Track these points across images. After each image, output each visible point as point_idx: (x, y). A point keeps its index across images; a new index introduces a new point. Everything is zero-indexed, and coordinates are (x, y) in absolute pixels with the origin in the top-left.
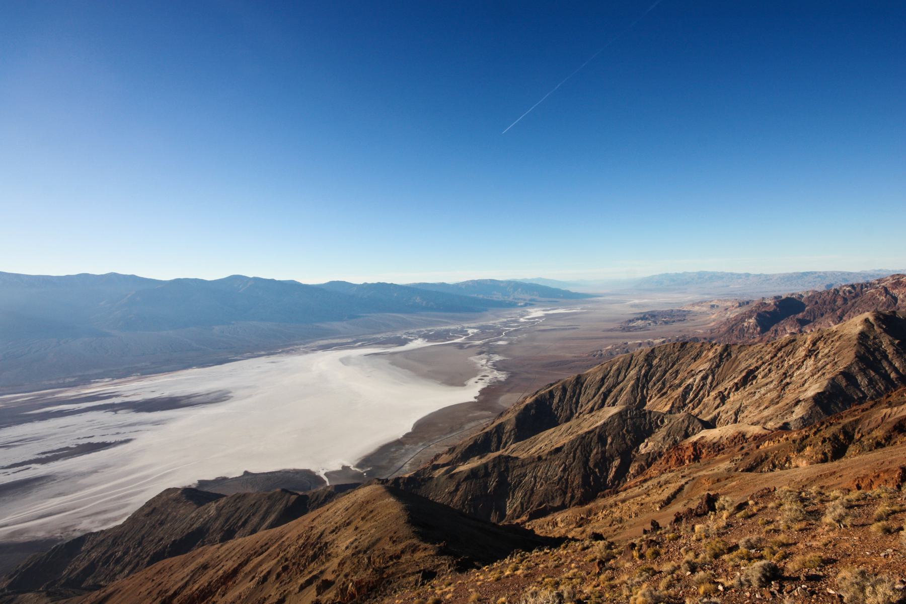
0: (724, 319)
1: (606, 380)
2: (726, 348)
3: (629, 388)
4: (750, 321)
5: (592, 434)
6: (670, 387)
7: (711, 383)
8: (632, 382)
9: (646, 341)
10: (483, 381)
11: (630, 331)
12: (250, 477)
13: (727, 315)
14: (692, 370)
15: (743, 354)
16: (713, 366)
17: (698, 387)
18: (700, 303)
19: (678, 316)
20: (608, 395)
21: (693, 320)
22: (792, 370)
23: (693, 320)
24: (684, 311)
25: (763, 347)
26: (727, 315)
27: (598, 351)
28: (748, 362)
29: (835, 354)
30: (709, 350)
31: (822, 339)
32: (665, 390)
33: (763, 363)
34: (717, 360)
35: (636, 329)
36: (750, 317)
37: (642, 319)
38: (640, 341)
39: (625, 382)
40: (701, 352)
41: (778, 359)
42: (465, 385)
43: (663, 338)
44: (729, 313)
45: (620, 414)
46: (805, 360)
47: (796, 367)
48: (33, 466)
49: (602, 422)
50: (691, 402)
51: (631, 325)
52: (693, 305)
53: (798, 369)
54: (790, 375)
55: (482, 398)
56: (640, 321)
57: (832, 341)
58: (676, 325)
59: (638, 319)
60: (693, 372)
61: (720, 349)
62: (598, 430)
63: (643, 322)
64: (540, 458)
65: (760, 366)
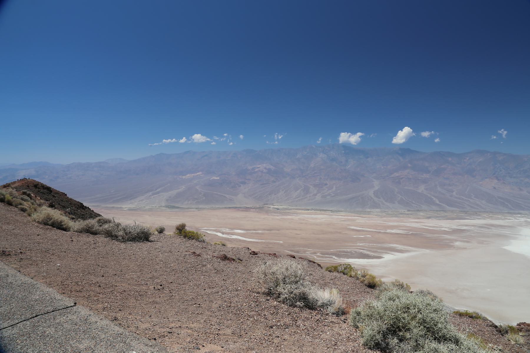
48: (334, 257)
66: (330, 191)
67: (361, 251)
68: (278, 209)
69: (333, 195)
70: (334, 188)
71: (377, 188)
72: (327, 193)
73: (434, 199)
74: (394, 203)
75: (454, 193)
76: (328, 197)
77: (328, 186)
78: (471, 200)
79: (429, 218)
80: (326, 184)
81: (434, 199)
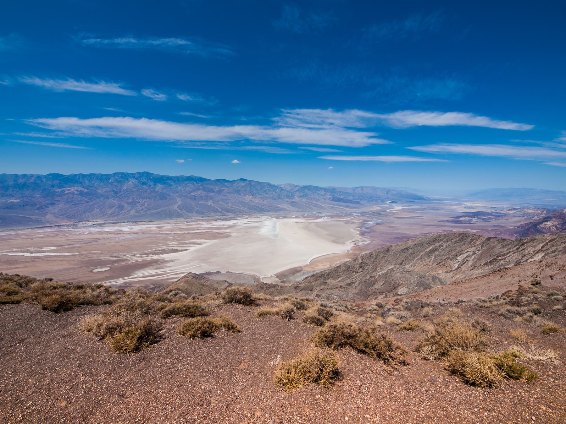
0: (531, 221)
1: (407, 250)
2: (489, 239)
3: (419, 257)
4: (546, 223)
5: (374, 278)
6: (445, 259)
7: (473, 260)
8: (423, 253)
9: (466, 230)
10: (355, 243)
11: (458, 223)
12: (230, 274)
13: (534, 218)
14: (462, 251)
15: (500, 244)
16: (477, 250)
17: (463, 262)
18: (514, 209)
19: (499, 215)
20: (406, 259)
21: (507, 220)
22: (526, 258)
23: (507, 220)
24: (502, 214)
25: (514, 242)
26: (534, 218)
27: (431, 233)
28: (501, 250)
29: (560, 251)
30: (477, 240)
31: (556, 240)
32: (441, 261)
33: (510, 252)
34: (480, 246)
35: (461, 222)
36: (547, 221)
37: (469, 217)
38: (462, 230)
39: (418, 253)
40: (472, 240)
41: (521, 250)
42: (344, 244)
43: (478, 229)
44: (536, 217)
45: (392, 270)
46: (537, 253)
47: (530, 256)
48: (151, 255)
49: (381, 273)
50: (454, 270)
51: (461, 219)
52: (509, 210)
53: (532, 257)
54: (524, 262)
55: (351, 252)
56: (467, 217)
57: (562, 243)
58: (493, 222)
59: (466, 216)
60: (463, 252)
61: (484, 239)
62: (377, 277)
63: (469, 218)
64: (341, 287)
65: (508, 253)
66: (143, 207)
67: (172, 247)
68: (94, 224)
69: (146, 210)
70: (146, 205)
71: (179, 203)
72: (140, 209)
73: (218, 209)
74: (193, 213)
75: (230, 205)
76: (142, 212)
77: (140, 203)
78: (239, 208)
79: (216, 220)
80: (139, 202)
81: (218, 209)
